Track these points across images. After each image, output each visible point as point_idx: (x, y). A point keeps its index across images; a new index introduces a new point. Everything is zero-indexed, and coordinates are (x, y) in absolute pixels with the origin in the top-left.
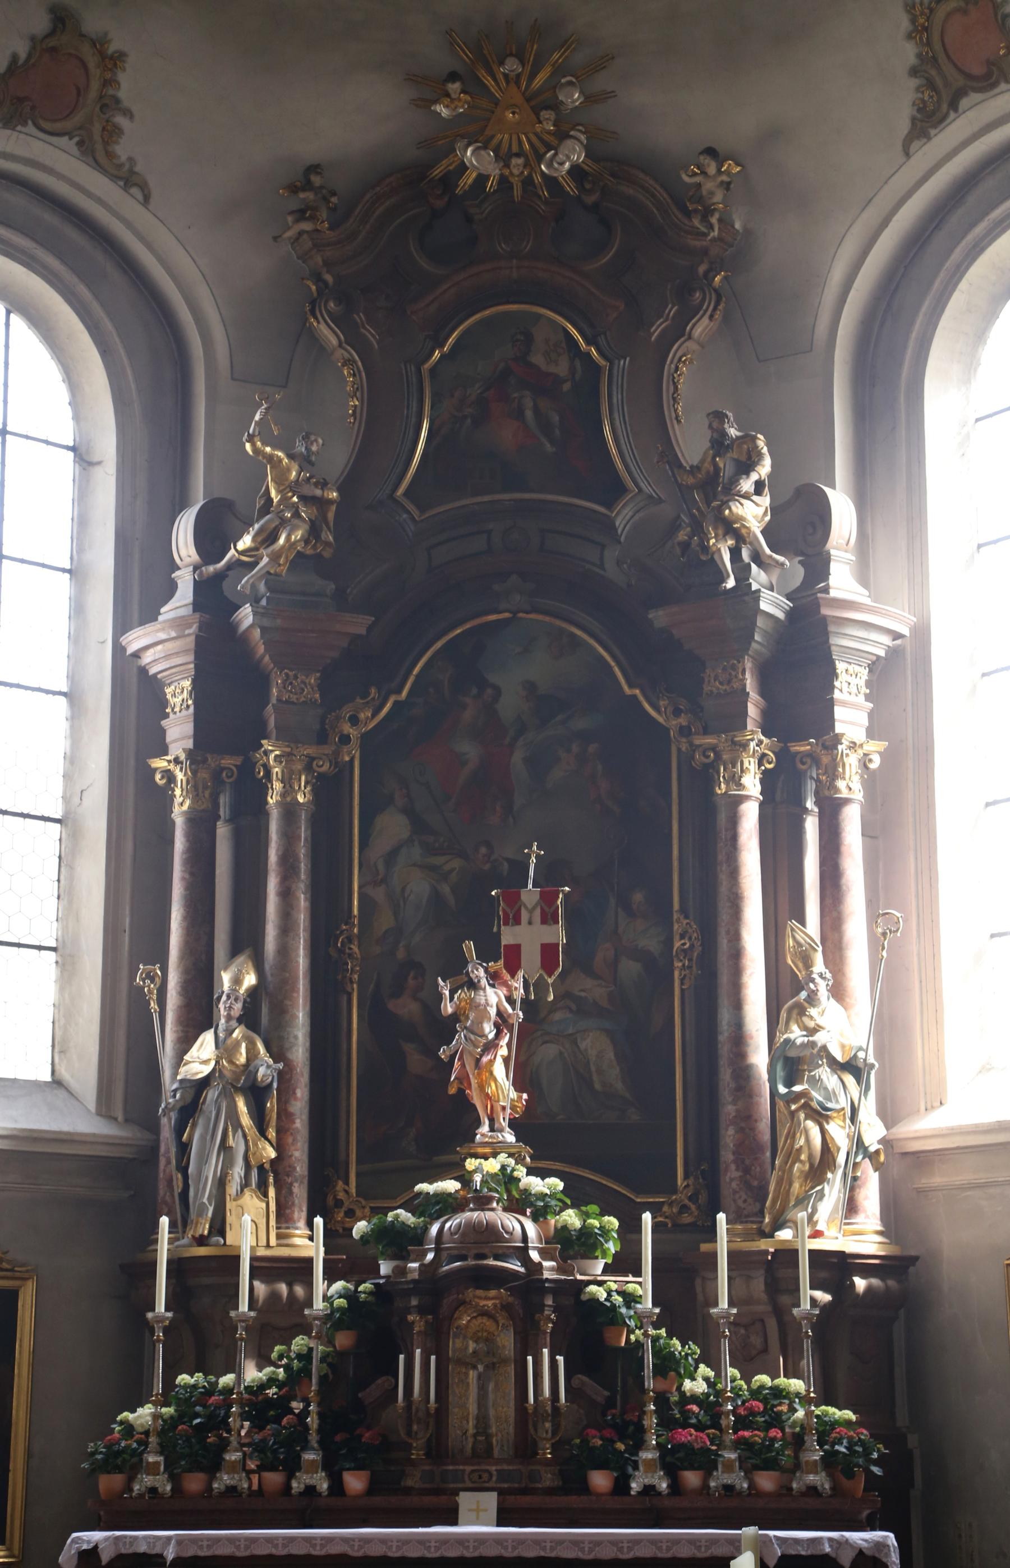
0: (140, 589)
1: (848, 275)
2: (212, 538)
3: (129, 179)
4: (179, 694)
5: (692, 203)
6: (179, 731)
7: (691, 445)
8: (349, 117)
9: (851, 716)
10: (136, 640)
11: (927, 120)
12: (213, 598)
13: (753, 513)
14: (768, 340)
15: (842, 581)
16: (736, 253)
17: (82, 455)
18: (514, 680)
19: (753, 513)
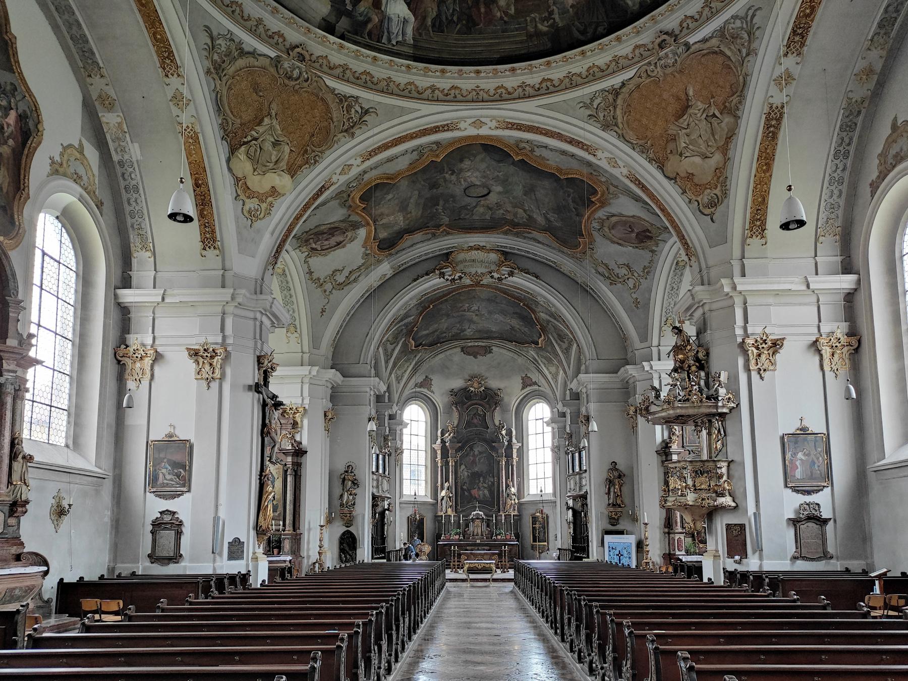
0: (433, 440)
1: (513, 403)
2: (443, 434)
3: (432, 392)
4: (439, 452)
5: (496, 394)
6: (439, 457)
7: (497, 423)
8: (458, 383)
9: (515, 456)
10: (434, 446)
11: (523, 388)
12: (443, 442)
13: (504, 432)
14: (505, 410)
15: (514, 440)
16: (502, 399)
17: (426, 422)
18: (476, 450)
19: (504, 432)
